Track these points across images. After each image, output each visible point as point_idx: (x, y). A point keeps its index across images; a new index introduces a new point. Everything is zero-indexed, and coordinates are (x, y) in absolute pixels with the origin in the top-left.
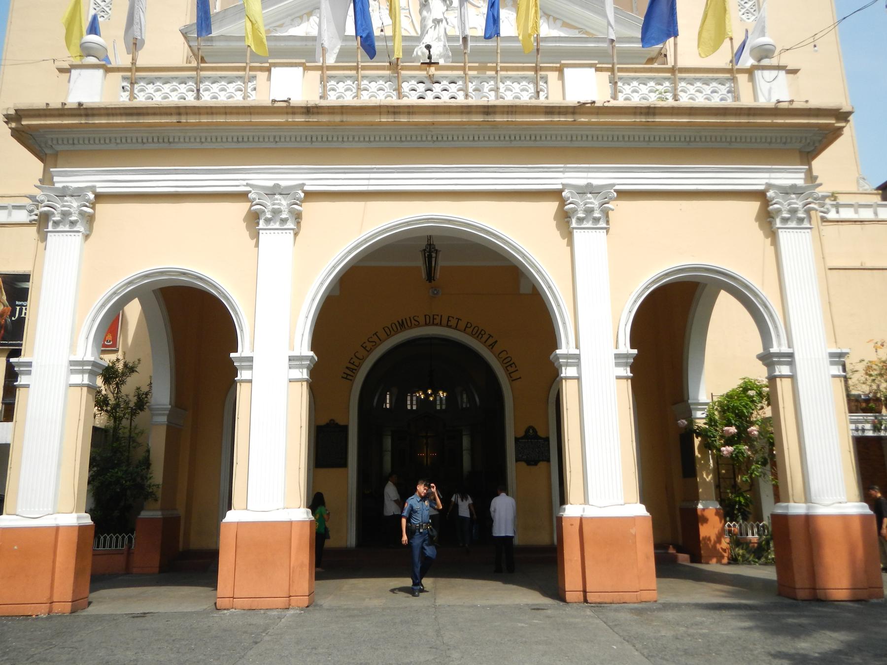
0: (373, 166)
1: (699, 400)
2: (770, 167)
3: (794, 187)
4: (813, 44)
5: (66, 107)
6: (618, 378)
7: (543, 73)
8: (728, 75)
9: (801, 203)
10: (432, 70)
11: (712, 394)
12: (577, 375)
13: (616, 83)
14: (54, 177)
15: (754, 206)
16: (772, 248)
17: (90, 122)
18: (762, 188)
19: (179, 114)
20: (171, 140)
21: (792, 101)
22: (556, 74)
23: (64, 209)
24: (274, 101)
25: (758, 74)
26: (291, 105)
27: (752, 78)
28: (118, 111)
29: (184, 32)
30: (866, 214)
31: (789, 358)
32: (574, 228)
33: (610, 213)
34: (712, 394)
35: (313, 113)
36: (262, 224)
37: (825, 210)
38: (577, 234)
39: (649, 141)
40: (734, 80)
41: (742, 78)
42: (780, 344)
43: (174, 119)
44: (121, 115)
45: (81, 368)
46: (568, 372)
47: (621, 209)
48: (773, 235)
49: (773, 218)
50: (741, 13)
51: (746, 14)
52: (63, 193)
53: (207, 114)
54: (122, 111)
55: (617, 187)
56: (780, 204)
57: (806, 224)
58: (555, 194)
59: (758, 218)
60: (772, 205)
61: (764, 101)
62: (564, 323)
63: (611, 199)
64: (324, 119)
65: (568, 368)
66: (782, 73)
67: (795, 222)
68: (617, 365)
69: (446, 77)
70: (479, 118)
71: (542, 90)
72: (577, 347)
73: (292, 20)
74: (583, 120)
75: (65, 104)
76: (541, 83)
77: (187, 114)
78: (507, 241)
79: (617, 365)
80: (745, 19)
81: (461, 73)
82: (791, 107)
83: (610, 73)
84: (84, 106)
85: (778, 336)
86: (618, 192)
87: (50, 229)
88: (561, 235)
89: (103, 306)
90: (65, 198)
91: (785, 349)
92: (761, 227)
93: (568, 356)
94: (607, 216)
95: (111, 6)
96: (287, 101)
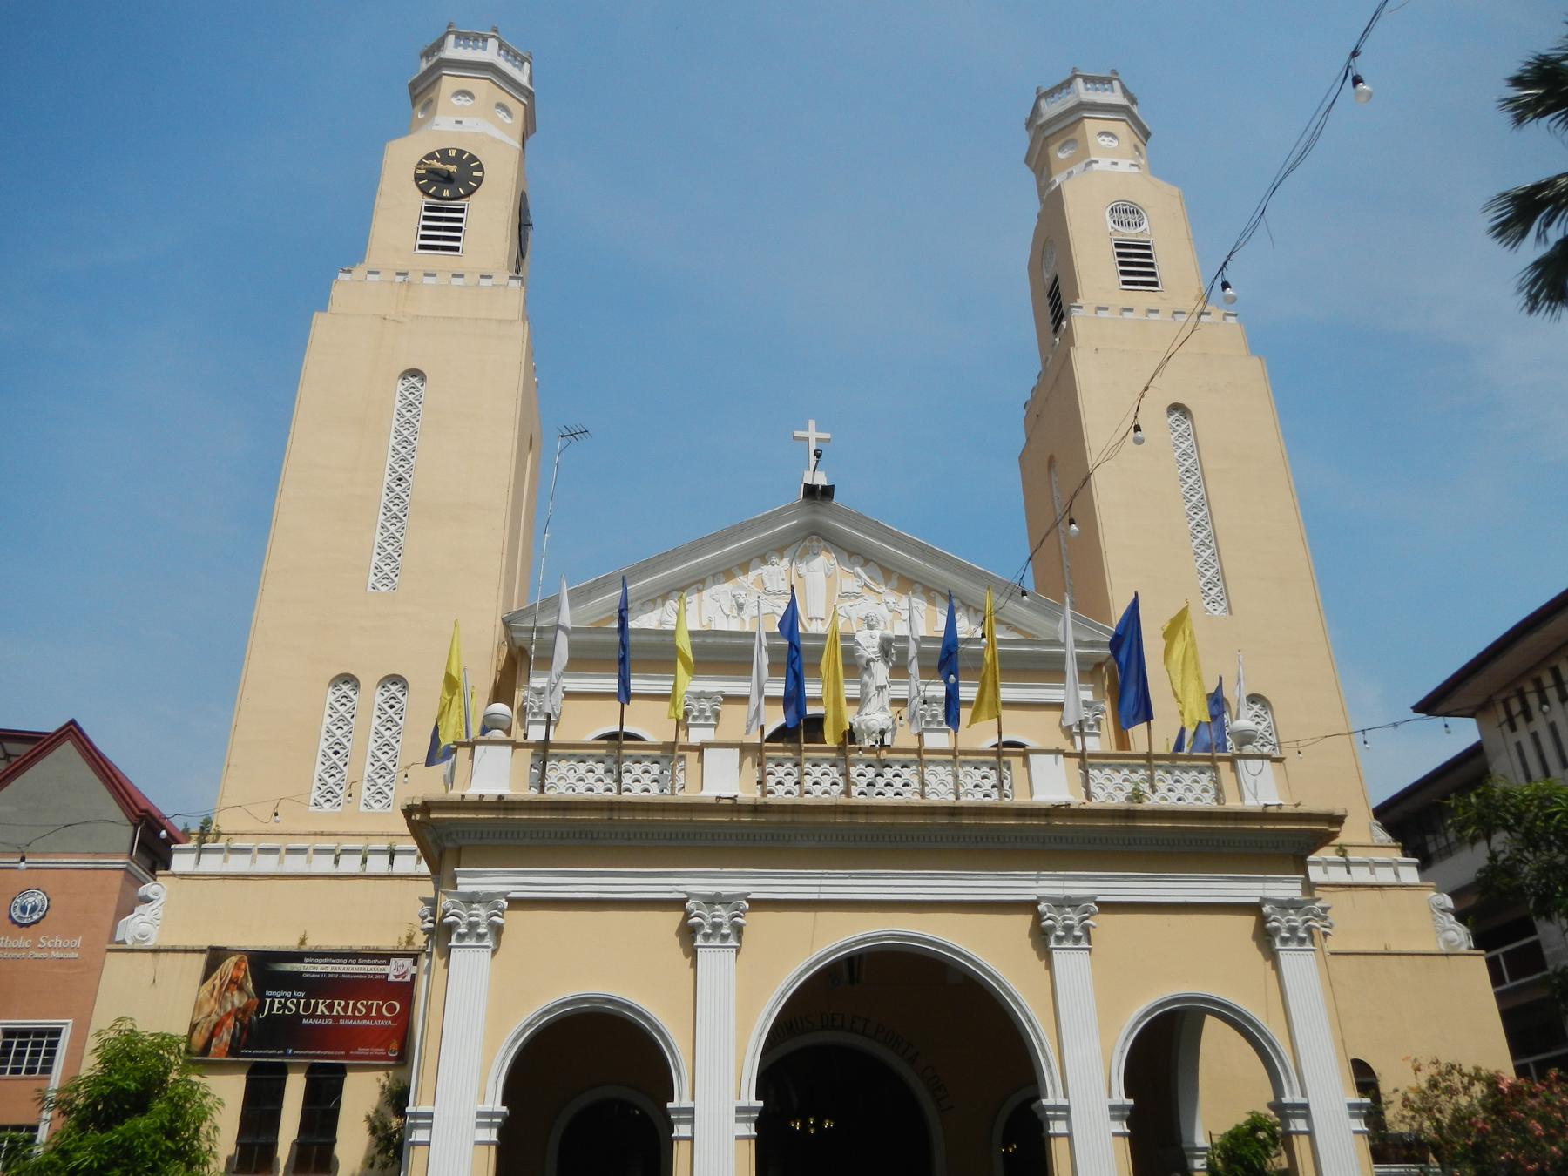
0: (825, 871)
1: (1195, 1144)
2: (1262, 876)
4: (1296, 750)
5: (484, 800)
6: (1115, 1134)
7: (1005, 758)
8: (1209, 763)
9: (1300, 920)
10: (884, 754)
11: (1210, 1133)
12: (1066, 1132)
13: (1088, 771)
15: (1249, 921)
16: (1274, 972)
17: (510, 817)
18: (1256, 900)
19: (611, 810)
20: (595, 836)
21: (1280, 806)
22: (1020, 759)
23: (472, 919)
24: (719, 798)
25: (1241, 763)
26: (738, 803)
27: (1234, 768)
29: (507, 620)
30: (1385, 876)
31: (1304, 1110)
32: (1052, 949)
33: (1091, 929)
34: (1210, 1133)
35: (761, 812)
36: (699, 941)
37: (1328, 925)
38: (1056, 955)
39: (1129, 844)
40: (1215, 768)
41: (1224, 767)
42: (1292, 1093)
43: (605, 816)
45: (489, 1120)
46: (1057, 1127)
47: (1103, 924)
48: (1272, 956)
49: (1270, 936)
50: (1205, 602)
51: (1211, 603)
52: (470, 899)
53: (643, 810)
55: (1100, 899)
56: (1277, 921)
57: (1308, 946)
58: (1030, 906)
59: (1255, 937)
60: (1270, 922)
61: (1251, 803)
62: (1049, 1066)
63: (1092, 914)
64: (774, 818)
65: (1057, 1123)
66: (1267, 763)
67: (1296, 943)
68: (1113, 1118)
69: (897, 761)
70: (944, 820)
71: (1005, 778)
72: (1066, 1096)
73: (643, 604)
74: (1057, 823)
75: (483, 796)
76: (1005, 770)
77: (620, 810)
78: (978, 964)
79: (1113, 1118)
80: (1211, 610)
81: (914, 757)
82: (1280, 811)
83: (1079, 760)
84: (505, 800)
85: (1289, 1082)
86: (1098, 904)
87: (453, 943)
88: (1038, 955)
89: (515, 1040)
90: (474, 906)
91: (1299, 1099)
92: (1260, 947)
93: (1055, 1108)
94: (1088, 933)
95: (397, 572)
96: (734, 798)
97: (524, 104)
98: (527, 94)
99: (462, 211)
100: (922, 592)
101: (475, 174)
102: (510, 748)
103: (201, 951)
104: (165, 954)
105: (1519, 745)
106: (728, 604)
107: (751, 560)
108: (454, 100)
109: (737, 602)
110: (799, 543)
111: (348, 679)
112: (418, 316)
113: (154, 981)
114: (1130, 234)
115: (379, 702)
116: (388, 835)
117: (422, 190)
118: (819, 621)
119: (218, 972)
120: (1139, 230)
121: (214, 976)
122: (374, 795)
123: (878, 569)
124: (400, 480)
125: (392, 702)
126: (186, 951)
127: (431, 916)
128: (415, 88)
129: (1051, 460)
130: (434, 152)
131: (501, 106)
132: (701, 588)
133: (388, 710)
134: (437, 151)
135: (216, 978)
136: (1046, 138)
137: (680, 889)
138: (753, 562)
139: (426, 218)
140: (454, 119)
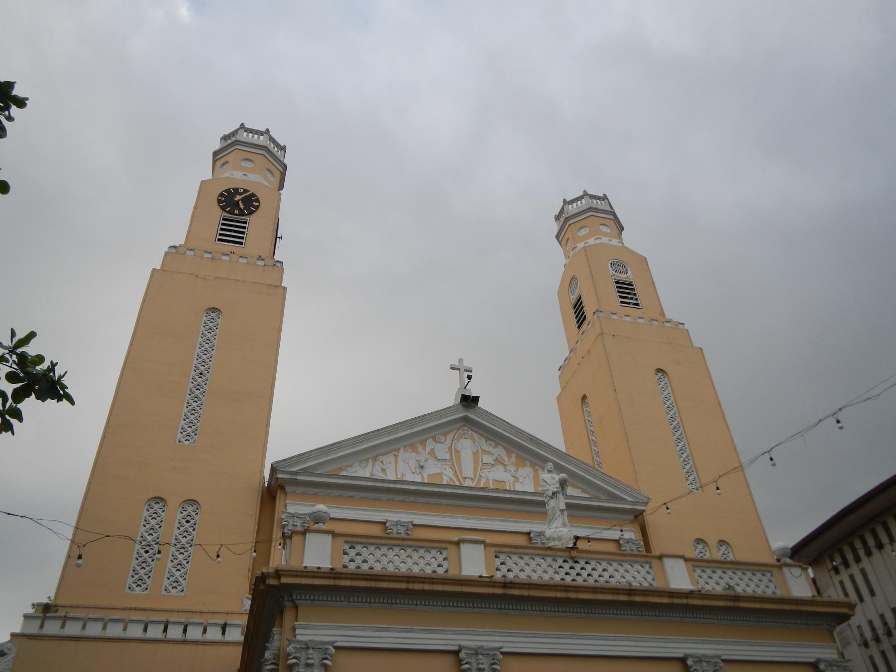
3: (834, 660)
10: (574, 553)
14: (297, 630)
24: (481, 577)
28: (361, 577)
44: (362, 579)
54: (365, 577)
55: (724, 657)
97: (281, 172)
98: (283, 167)
99: (246, 223)
100: (530, 466)
101: (254, 203)
102: (330, 536)
105: (841, 582)
106: (413, 464)
107: (427, 440)
108: (242, 164)
109: (420, 465)
110: (456, 431)
111: (159, 500)
112: (218, 277)
114: (622, 277)
115: (180, 518)
116: (183, 612)
117: (221, 209)
118: (470, 479)
120: (626, 276)
122: (172, 583)
123: (504, 451)
124: (201, 374)
125: (188, 518)
127: (274, 659)
128: (217, 156)
129: (584, 397)
130: (230, 189)
131: (269, 170)
132: (396, 454)
133: (185, 523)
134: (233, 189)
136: (570, 225)
137: (453, 642)
138: (428, 440)
139: (223, 224)
140: (242, 173)
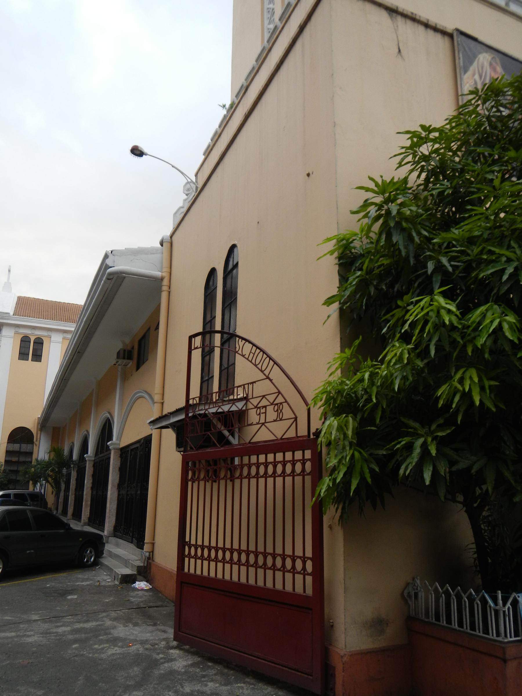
103: (443, 33)
104: (403, 19)
113: (399, 51)
119: (475, 64)
121: (471, 69)
126: (427, 25)
135: (474, 75)
